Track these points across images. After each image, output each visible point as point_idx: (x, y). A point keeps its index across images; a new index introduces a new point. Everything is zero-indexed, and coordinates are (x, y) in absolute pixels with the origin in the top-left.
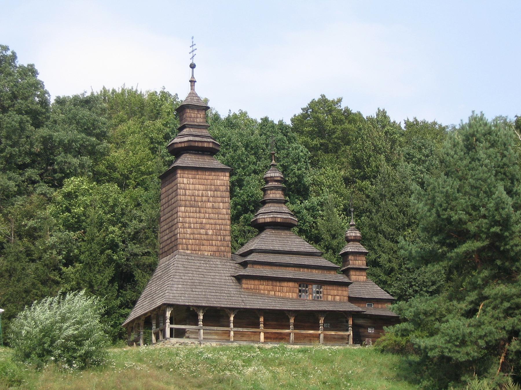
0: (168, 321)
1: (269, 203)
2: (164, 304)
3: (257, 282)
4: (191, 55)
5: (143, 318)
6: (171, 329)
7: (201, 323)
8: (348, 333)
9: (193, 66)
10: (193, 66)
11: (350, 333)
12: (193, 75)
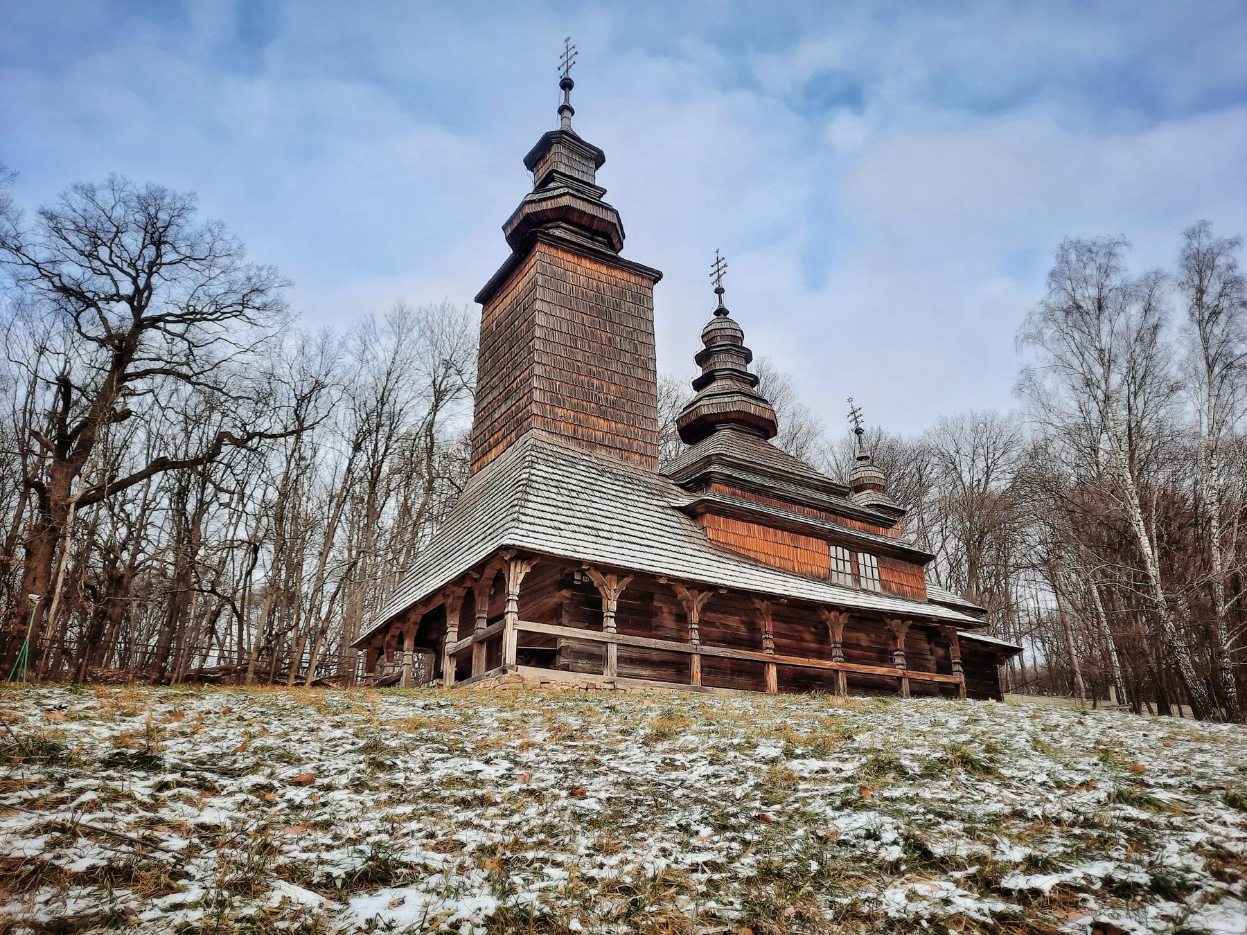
0: (513, 607)
1: (722, 378)
2: (506, 548)
3: (741, 527)
4: (564, 69)
5: (415, 617)
6: (524, 636)
7: (612, 622)
8: (958, 680)
9: (567, 85)
10: (567, 85)
11: (958, 677)
12: (567, 99)
